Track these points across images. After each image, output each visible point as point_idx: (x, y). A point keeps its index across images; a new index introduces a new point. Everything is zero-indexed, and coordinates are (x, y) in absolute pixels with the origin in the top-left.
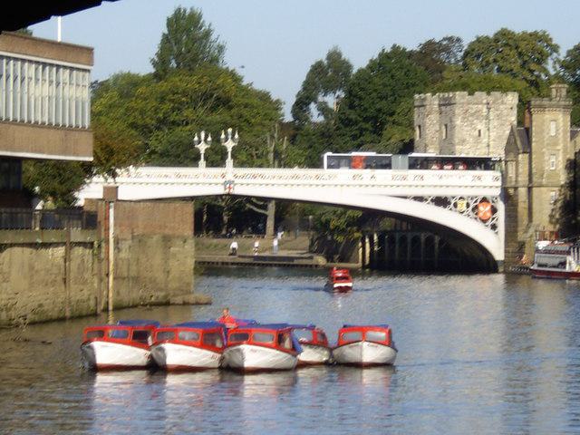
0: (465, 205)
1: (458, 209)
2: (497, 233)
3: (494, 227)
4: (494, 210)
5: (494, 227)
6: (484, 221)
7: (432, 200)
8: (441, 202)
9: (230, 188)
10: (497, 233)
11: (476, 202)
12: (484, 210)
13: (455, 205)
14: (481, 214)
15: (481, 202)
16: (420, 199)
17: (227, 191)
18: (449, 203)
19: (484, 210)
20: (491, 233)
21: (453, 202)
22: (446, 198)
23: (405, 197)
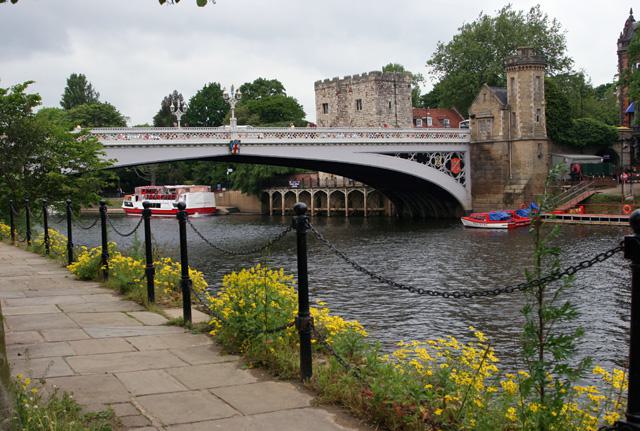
2: (464, 186)
3: (462, 180)
4: (462, 165)
5: (462, 180)
6: (455, 175)
8: (422, 158)
9: (236, 148)
12: (455, 163)
13: (433, 161)
16: (405, 156)
20: (459, 186)
21: (431, 157)
22: (426, 154)
23: (393, 154)
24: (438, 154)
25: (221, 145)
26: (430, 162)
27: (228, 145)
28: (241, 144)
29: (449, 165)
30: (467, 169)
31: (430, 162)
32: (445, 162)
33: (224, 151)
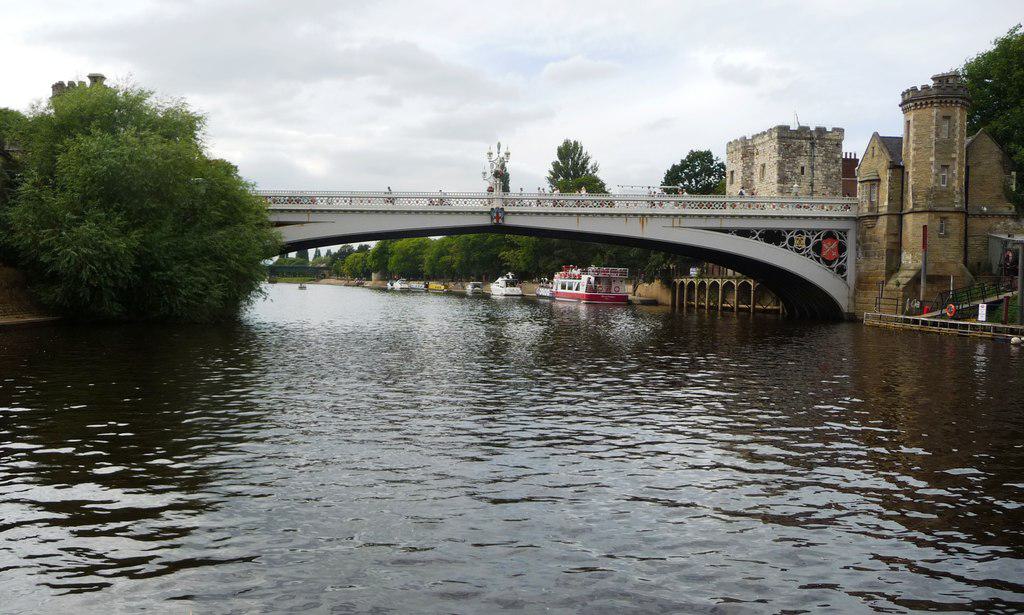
3: (841, 270)
4: (842, 249)
6: (828, 263)
7: (761, 236)
8: (773, 237)
9: (498, 218)
10: (845, 278)
11: (818, 237)
12: (829, 247)
13: (791, 241)
16: (744, 233)
17: (495, 221)
18: (784, 239)
19: (829, 247)
21: (788, 237)
22: (779, 232)
24: (800, 232)
25: (482, 213)
27: (489, 213)
28: (506, 213)
29: (818, 248)
33: (485, 221)
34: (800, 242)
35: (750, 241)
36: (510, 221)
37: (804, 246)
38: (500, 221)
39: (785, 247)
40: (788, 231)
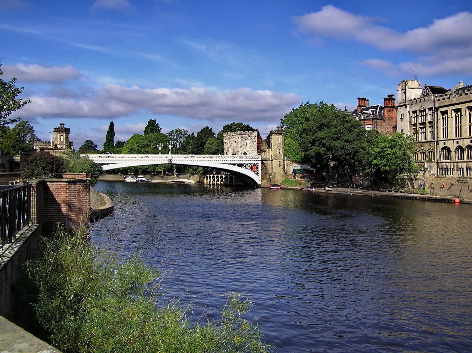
0: (248, 166)
1: (246, 167)
2: (258, 176)
3: (257, 173)
4: (257, 168)
5: (257, 173)
6: (254, 172)
8: (240, 165)
9: (170, 161)
10: (258, 176)
12: (254, 168)
13: (245, 166)
14: (253, 169)
15: (253, 165)
16: (234, 164)
17: (170, 162)
18: (243, 166)
21: (244, 165)
22: (242, 164)
23: (229, 164)
24: (247, 164)
26: (244, 167)
29: (252, 168)
30: (260, 169)
31: (244, 167)
32: (250, 166)
33: (167, 162)
34: (247, 167)
35: (235, 166)
36: (173, 162)
37: (248, 168)
38: (171, 162)
39: (244, 168)
40: (244, 164)
